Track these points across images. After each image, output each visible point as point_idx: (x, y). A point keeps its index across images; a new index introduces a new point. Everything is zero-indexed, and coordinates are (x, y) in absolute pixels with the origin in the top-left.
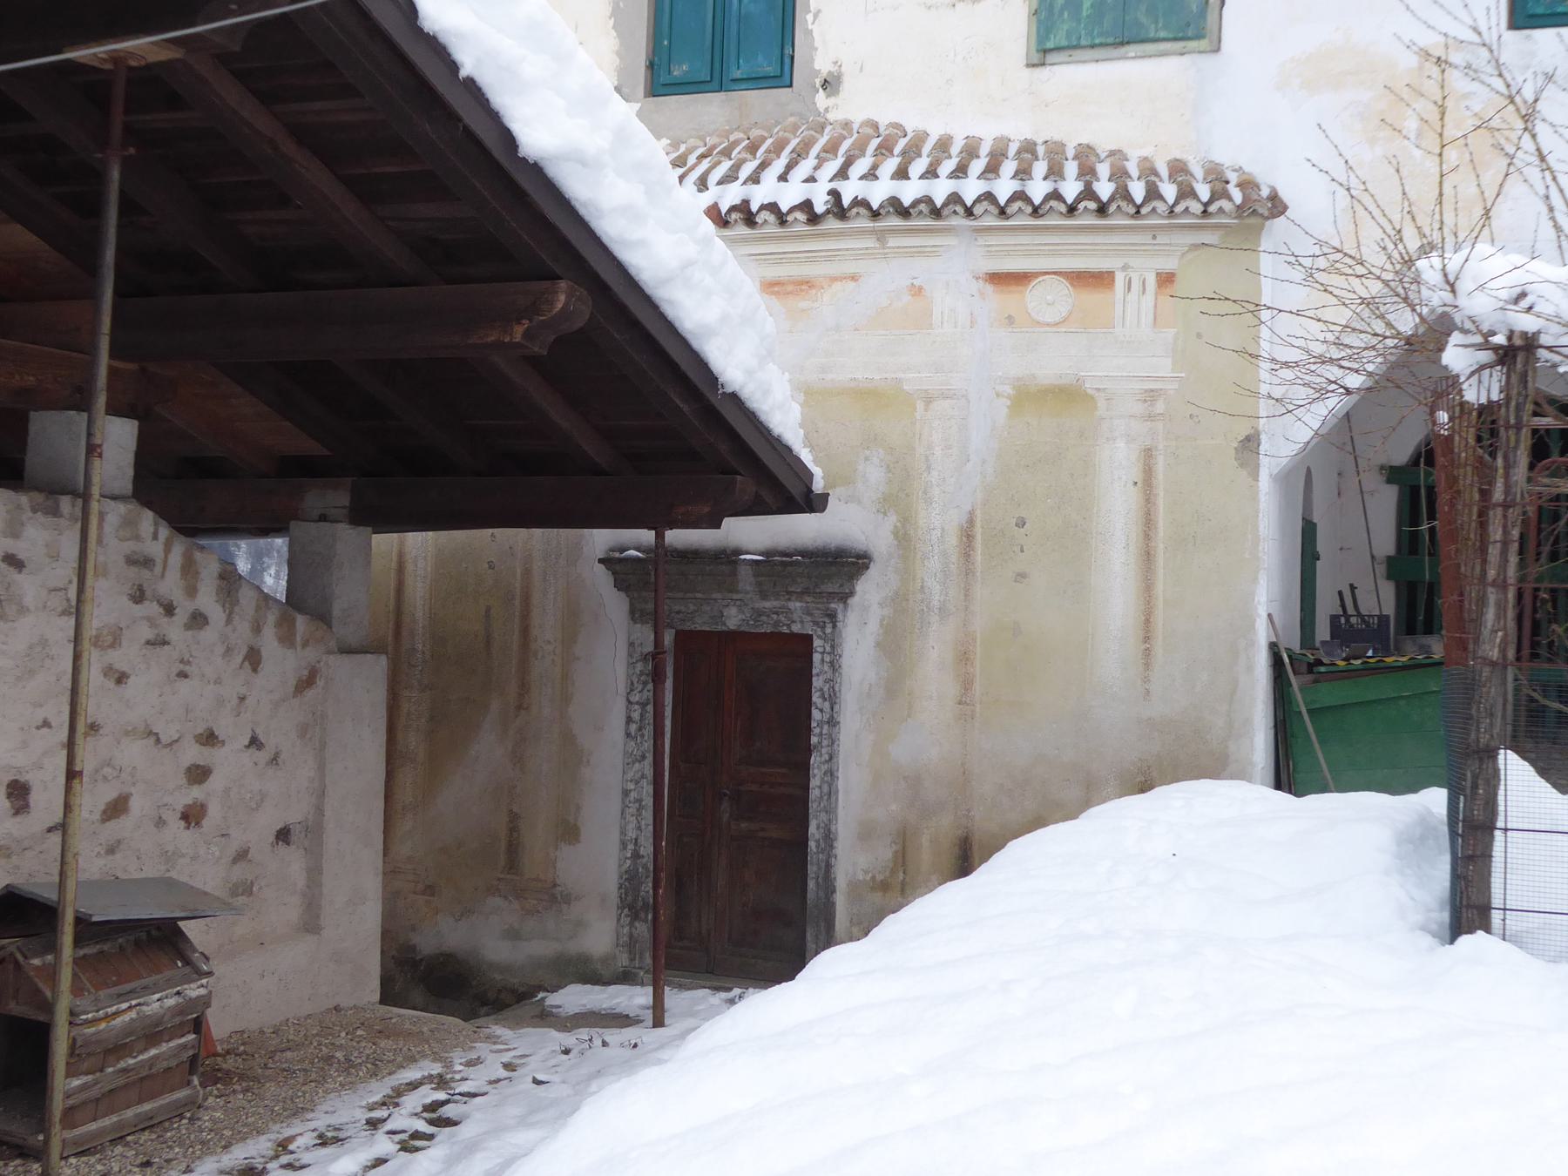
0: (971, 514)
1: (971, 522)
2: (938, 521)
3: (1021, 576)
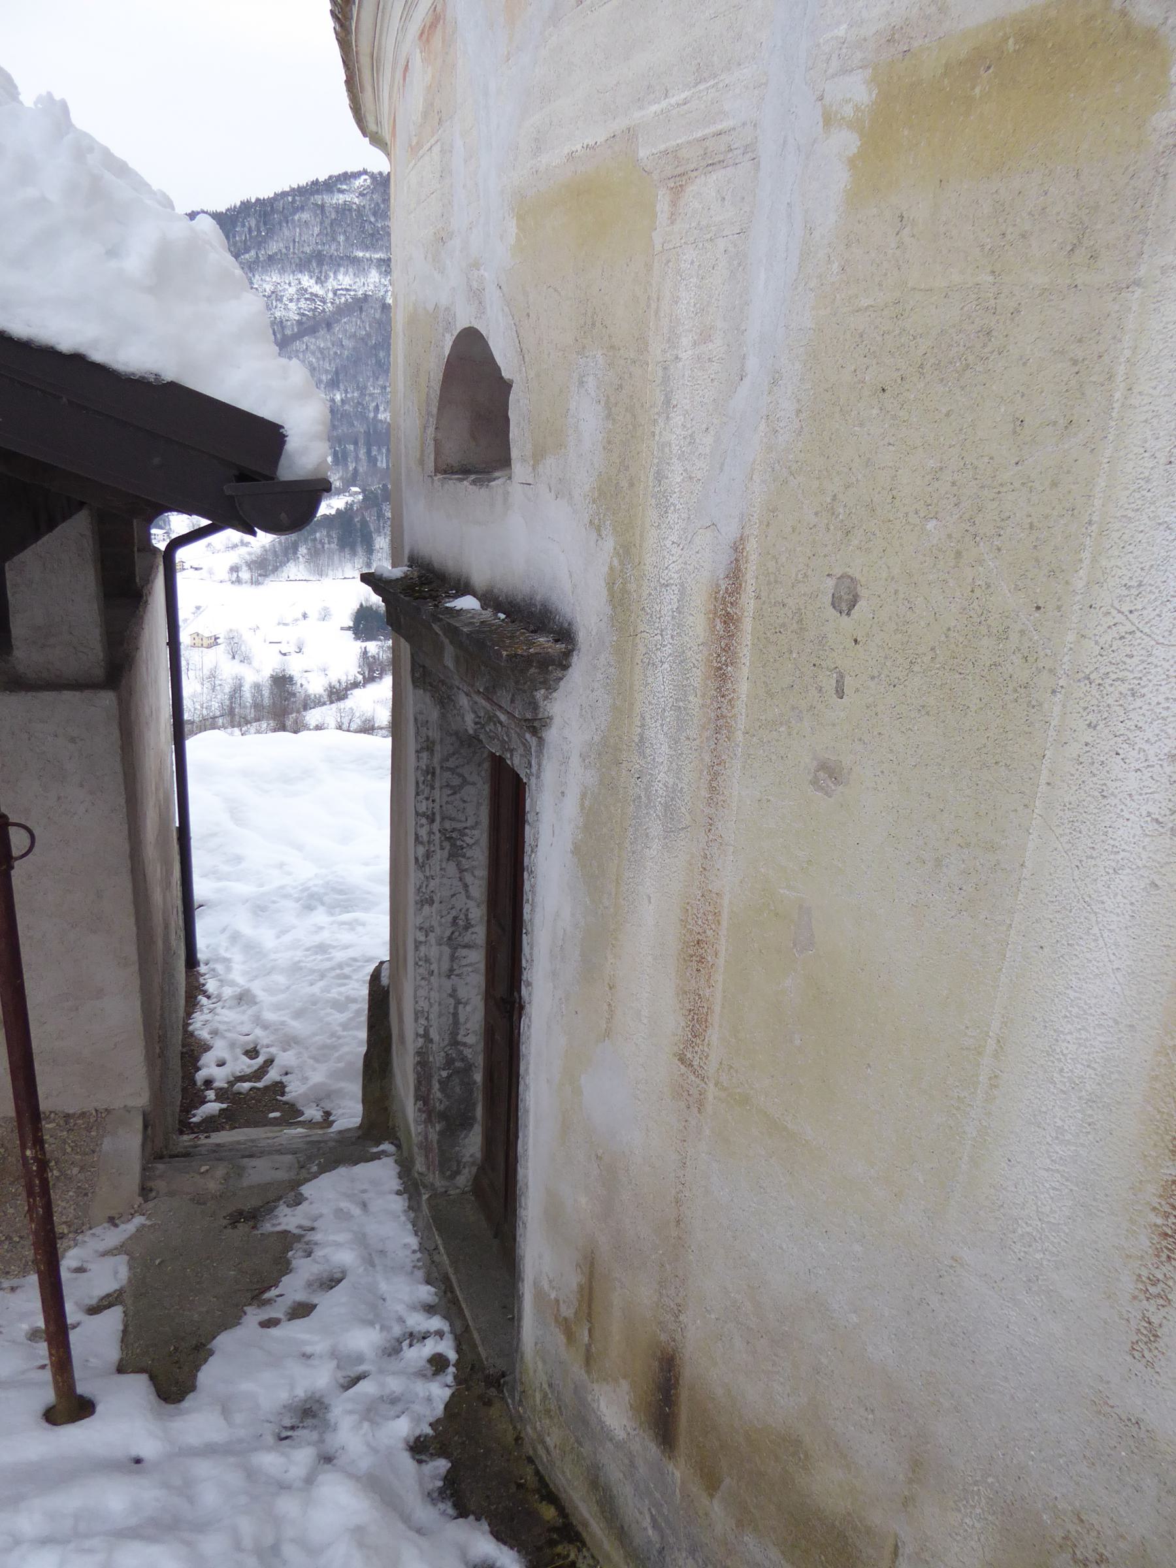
0: (738, 547)
1: (735, 575)
2: (682, 561)
3: (829, 773)
